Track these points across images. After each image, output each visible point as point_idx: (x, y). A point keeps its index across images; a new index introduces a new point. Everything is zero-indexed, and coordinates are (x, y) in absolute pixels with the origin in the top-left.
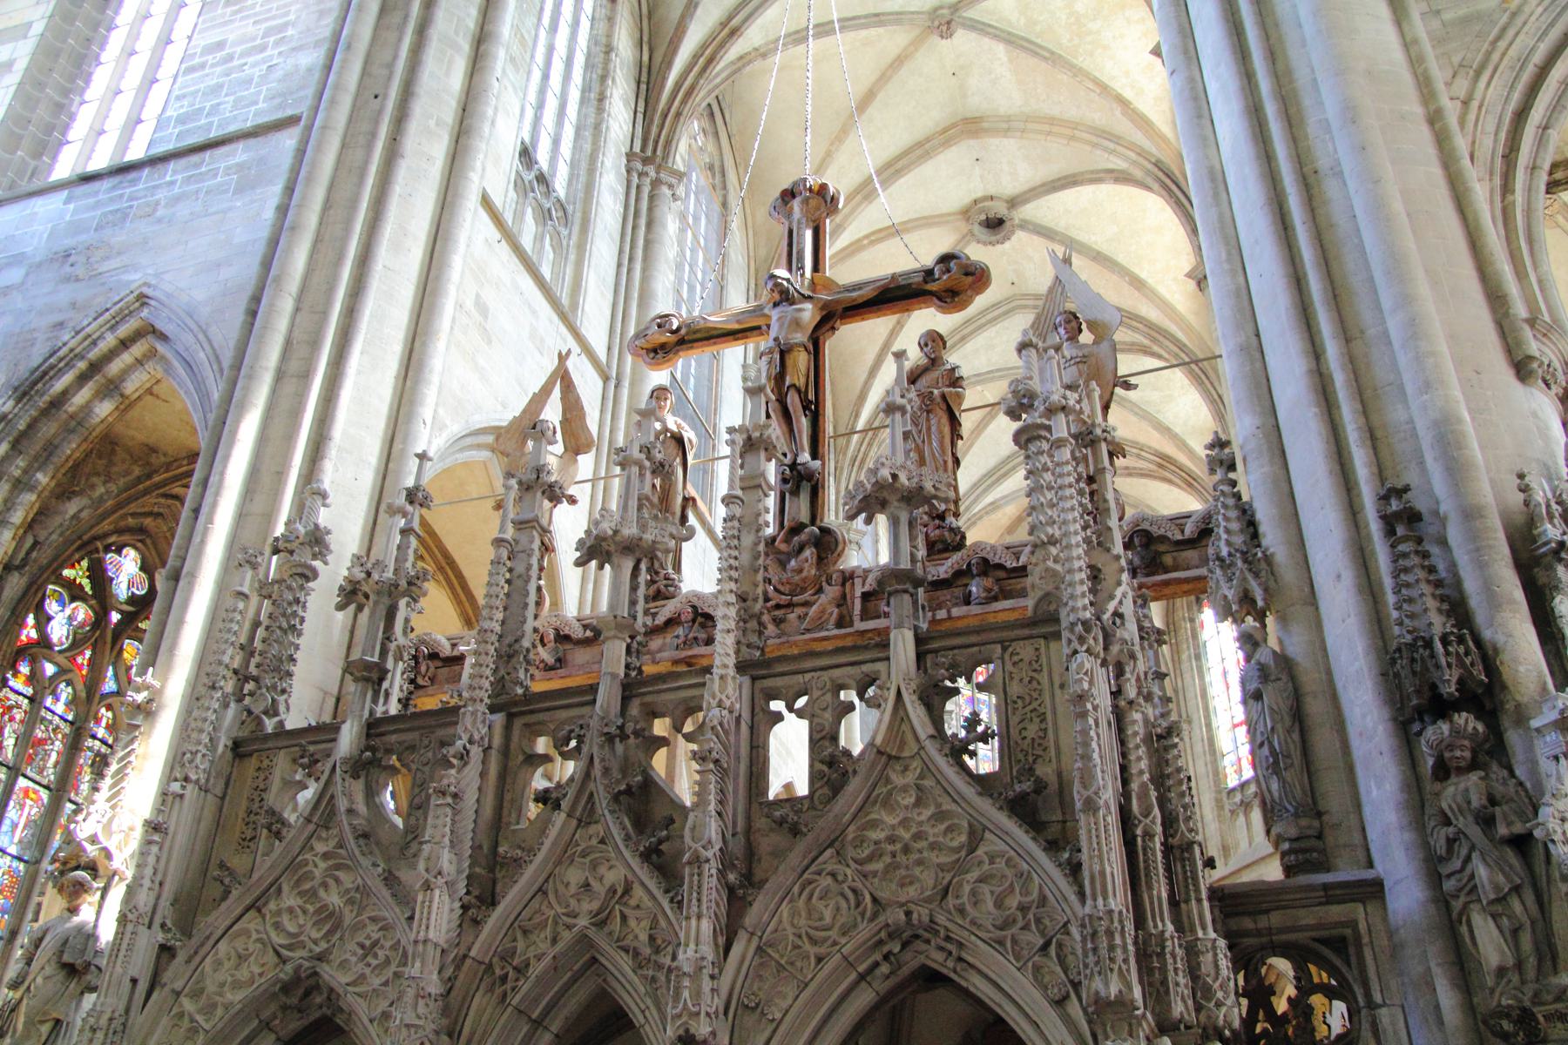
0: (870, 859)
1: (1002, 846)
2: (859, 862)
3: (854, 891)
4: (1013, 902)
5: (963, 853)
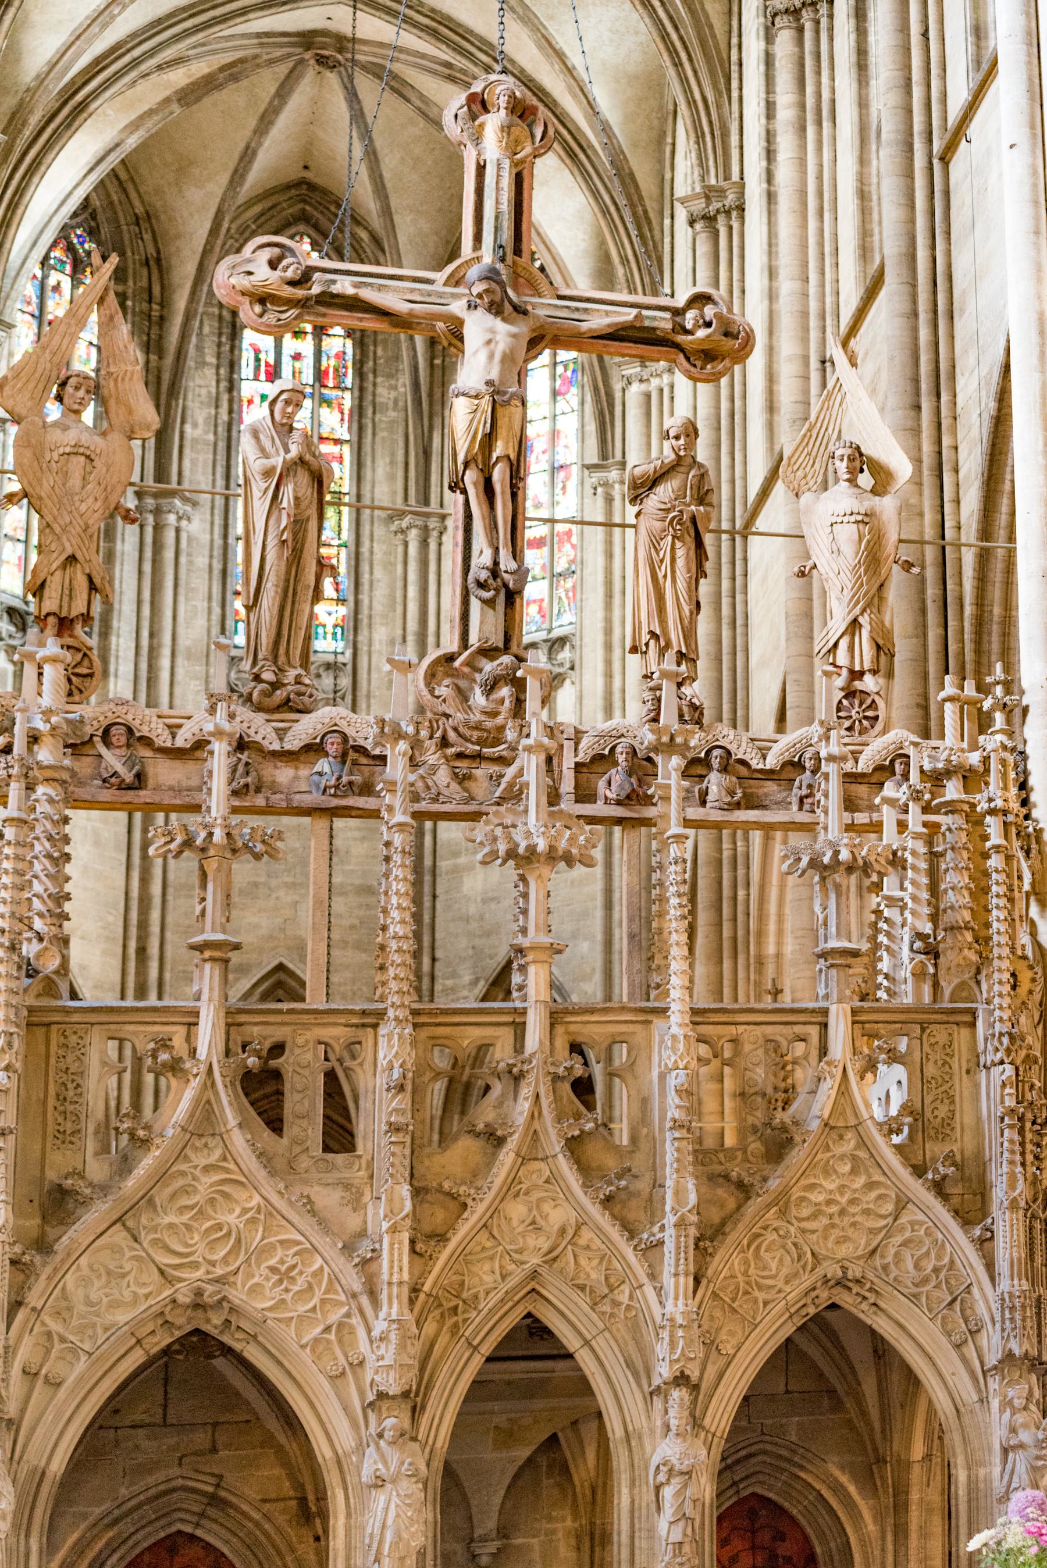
0: (807, 1219)
3: (795, 1244)
4: (929, 1266)
5: (890, 1220)
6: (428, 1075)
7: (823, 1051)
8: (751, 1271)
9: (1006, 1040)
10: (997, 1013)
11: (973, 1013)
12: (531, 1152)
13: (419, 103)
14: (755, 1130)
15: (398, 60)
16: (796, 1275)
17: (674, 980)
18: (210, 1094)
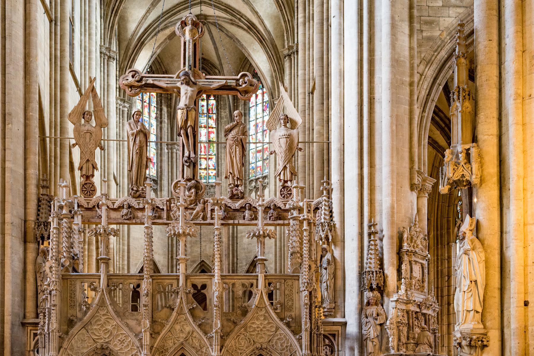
0: (252, 332)
1: (283, 332)
2: (250, 332)
6: (156, 292)
7: (257, 287)
8: (237, 345)
9: (306, 284)
10: (304, 276)
11: (298, 276)
12: (180, 313)
13: (226, 32)
14: (239, 307)
15: (219, 20)
16: (249, 346)
17: (216, 268)
18: (103, 296)
